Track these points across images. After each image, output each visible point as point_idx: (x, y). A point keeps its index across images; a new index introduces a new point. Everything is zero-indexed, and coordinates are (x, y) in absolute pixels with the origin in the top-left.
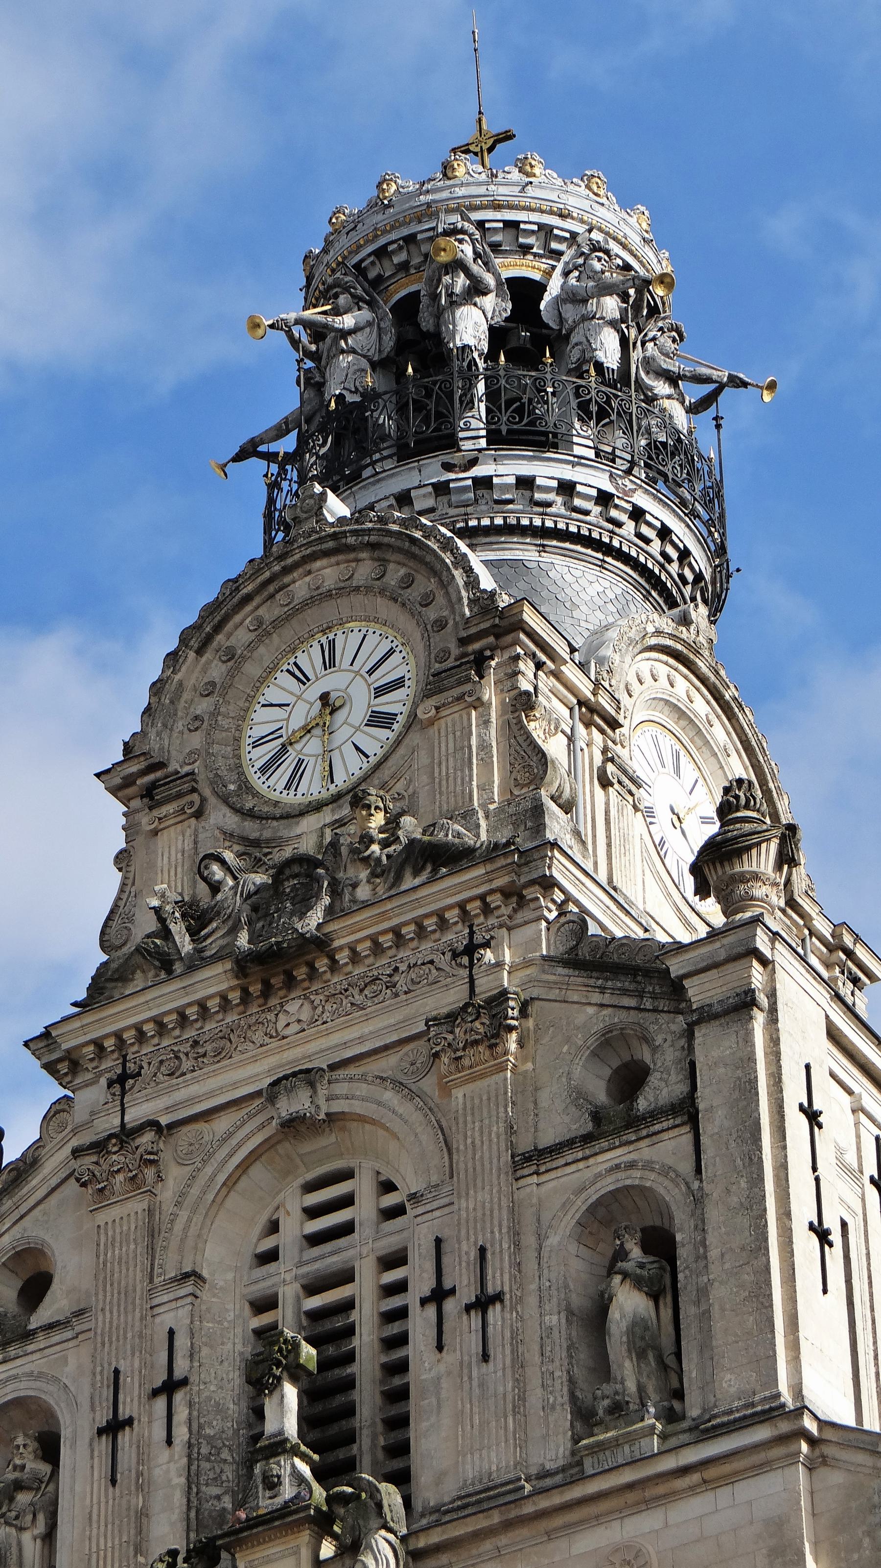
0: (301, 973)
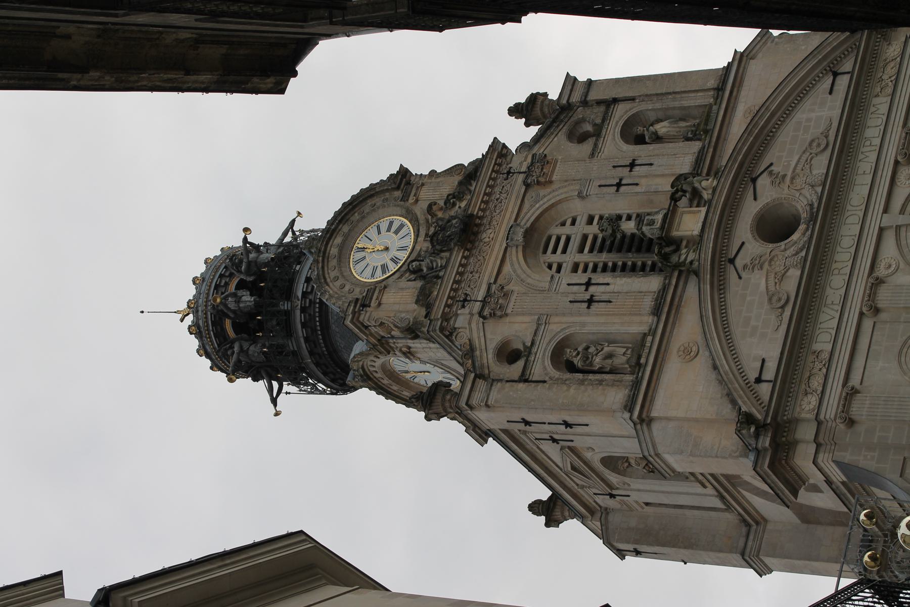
0: (476, 229)
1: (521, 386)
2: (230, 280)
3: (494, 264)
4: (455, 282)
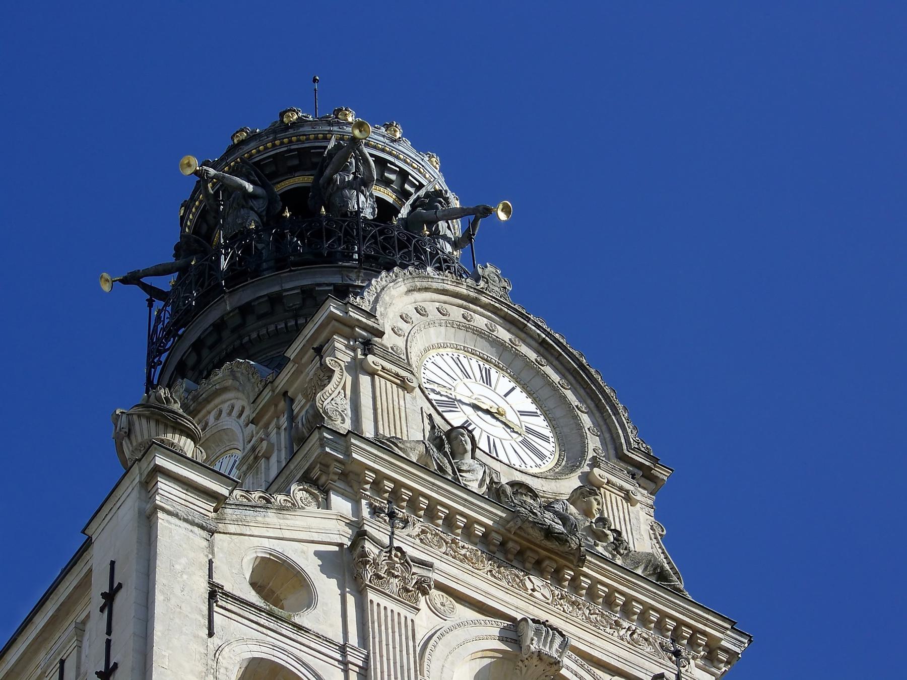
0: (550, 566)
1: (203, 588)
2: (394, 191)
3: (477, 589)
4: (433, 505)
